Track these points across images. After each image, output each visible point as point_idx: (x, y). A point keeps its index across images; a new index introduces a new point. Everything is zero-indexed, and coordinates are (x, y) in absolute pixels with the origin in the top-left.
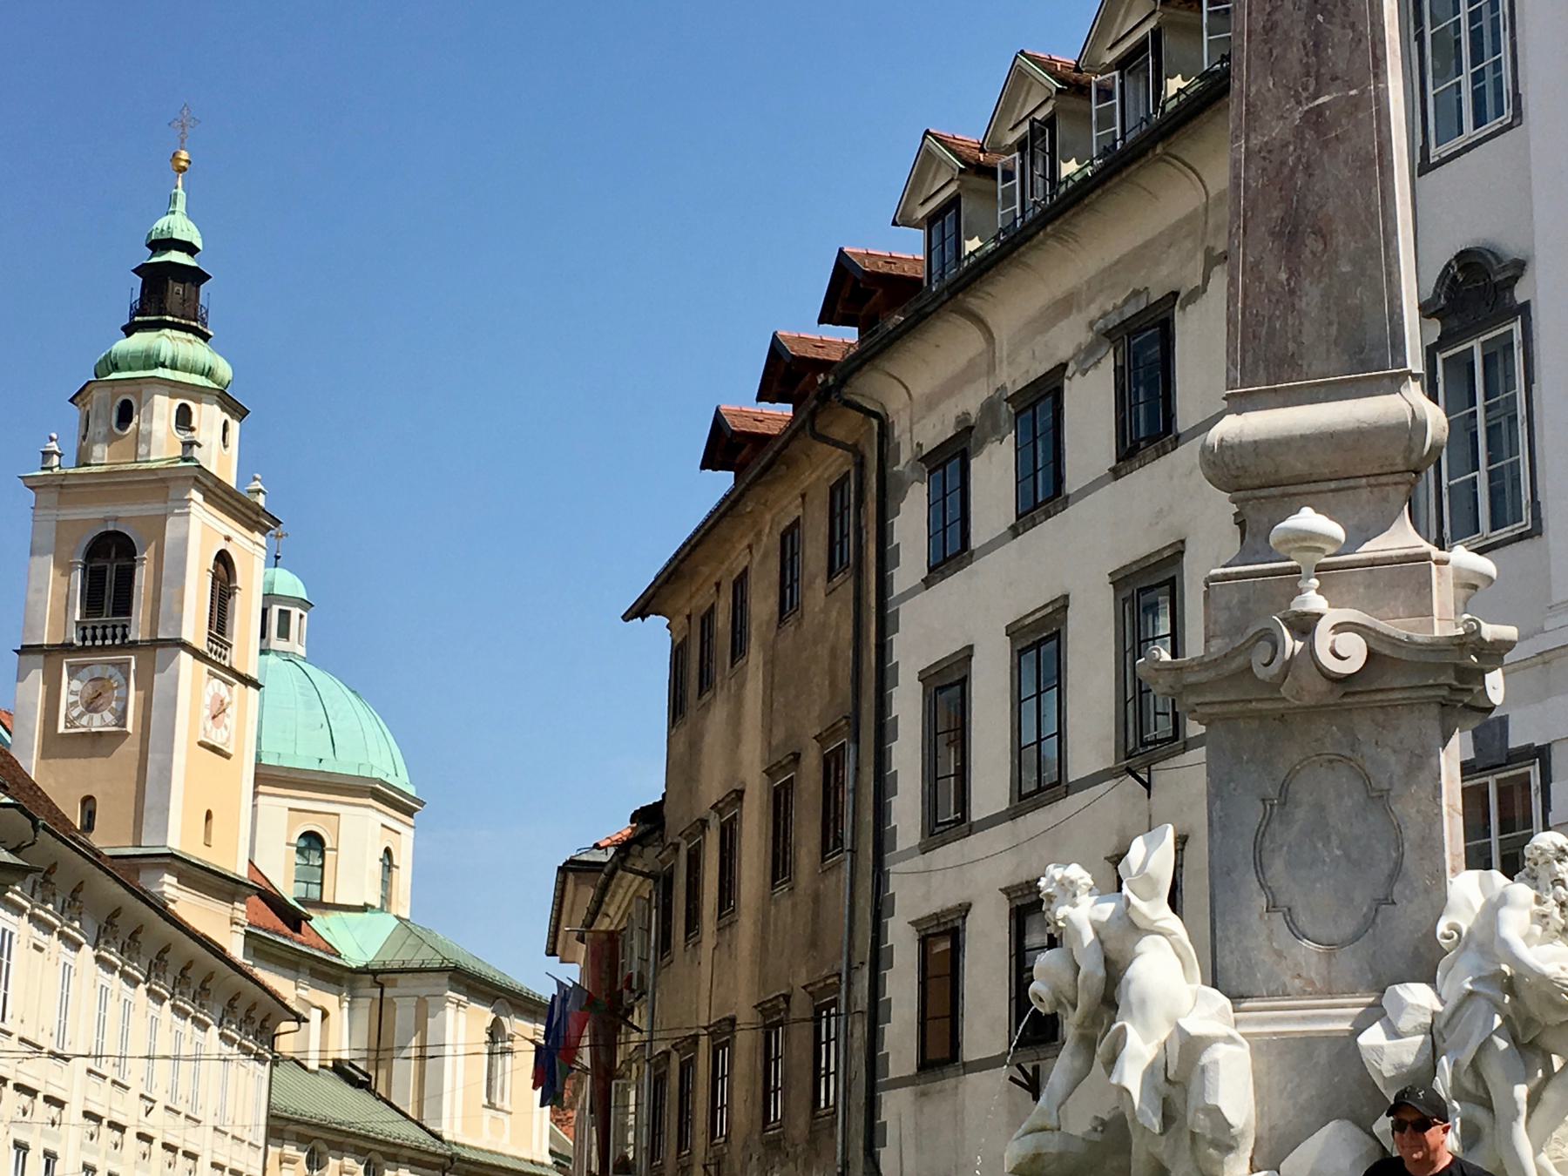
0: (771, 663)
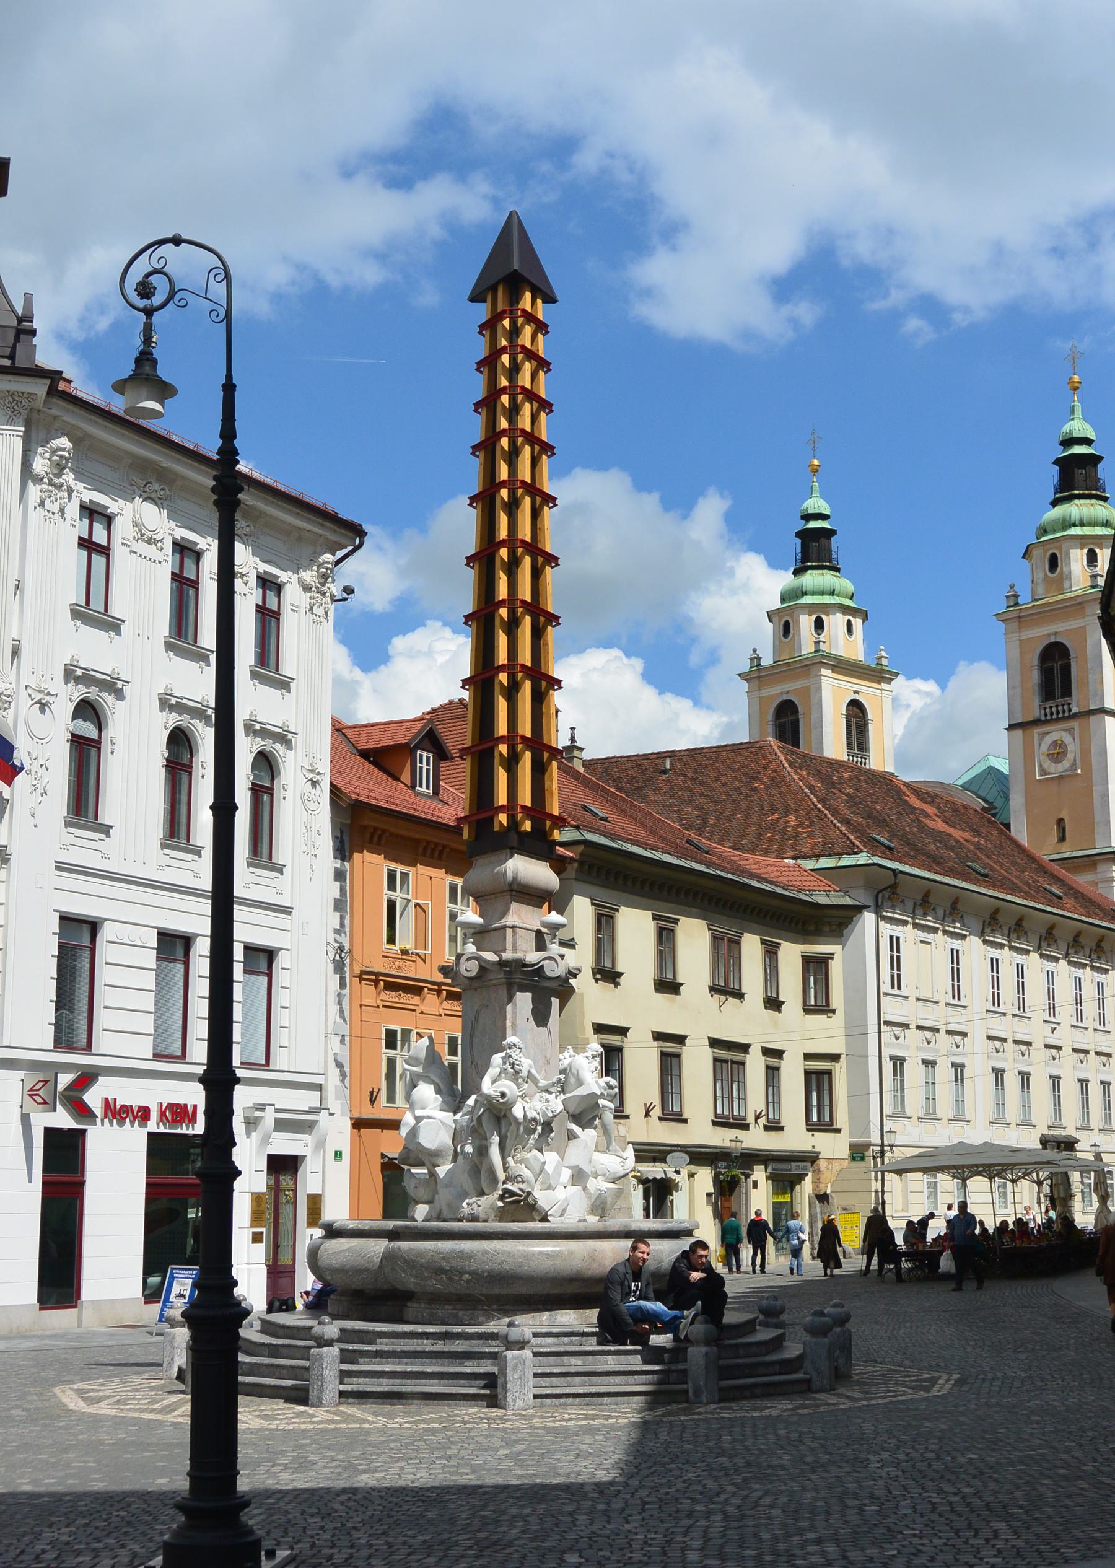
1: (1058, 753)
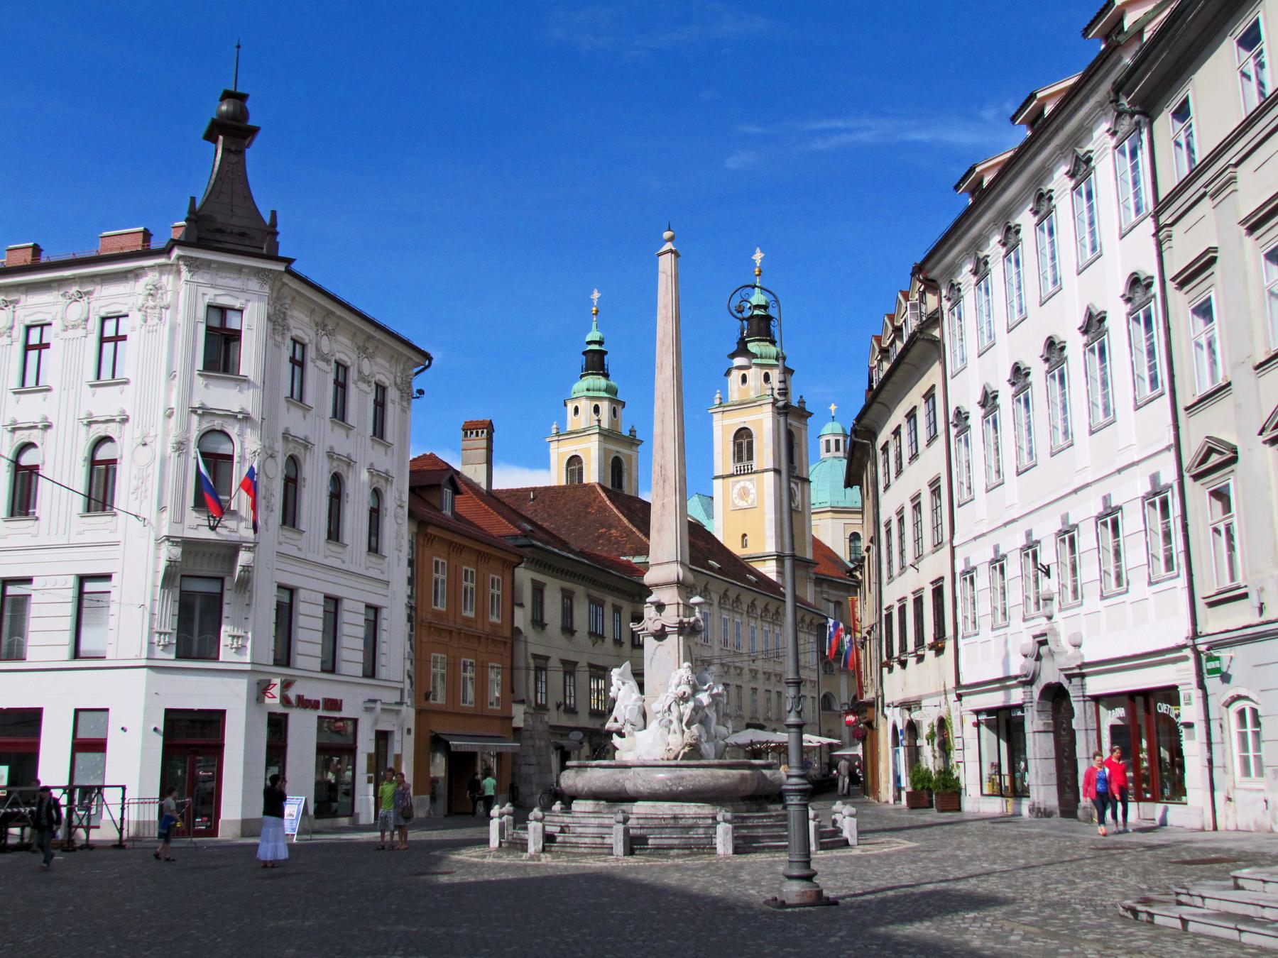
1: (744, 493)
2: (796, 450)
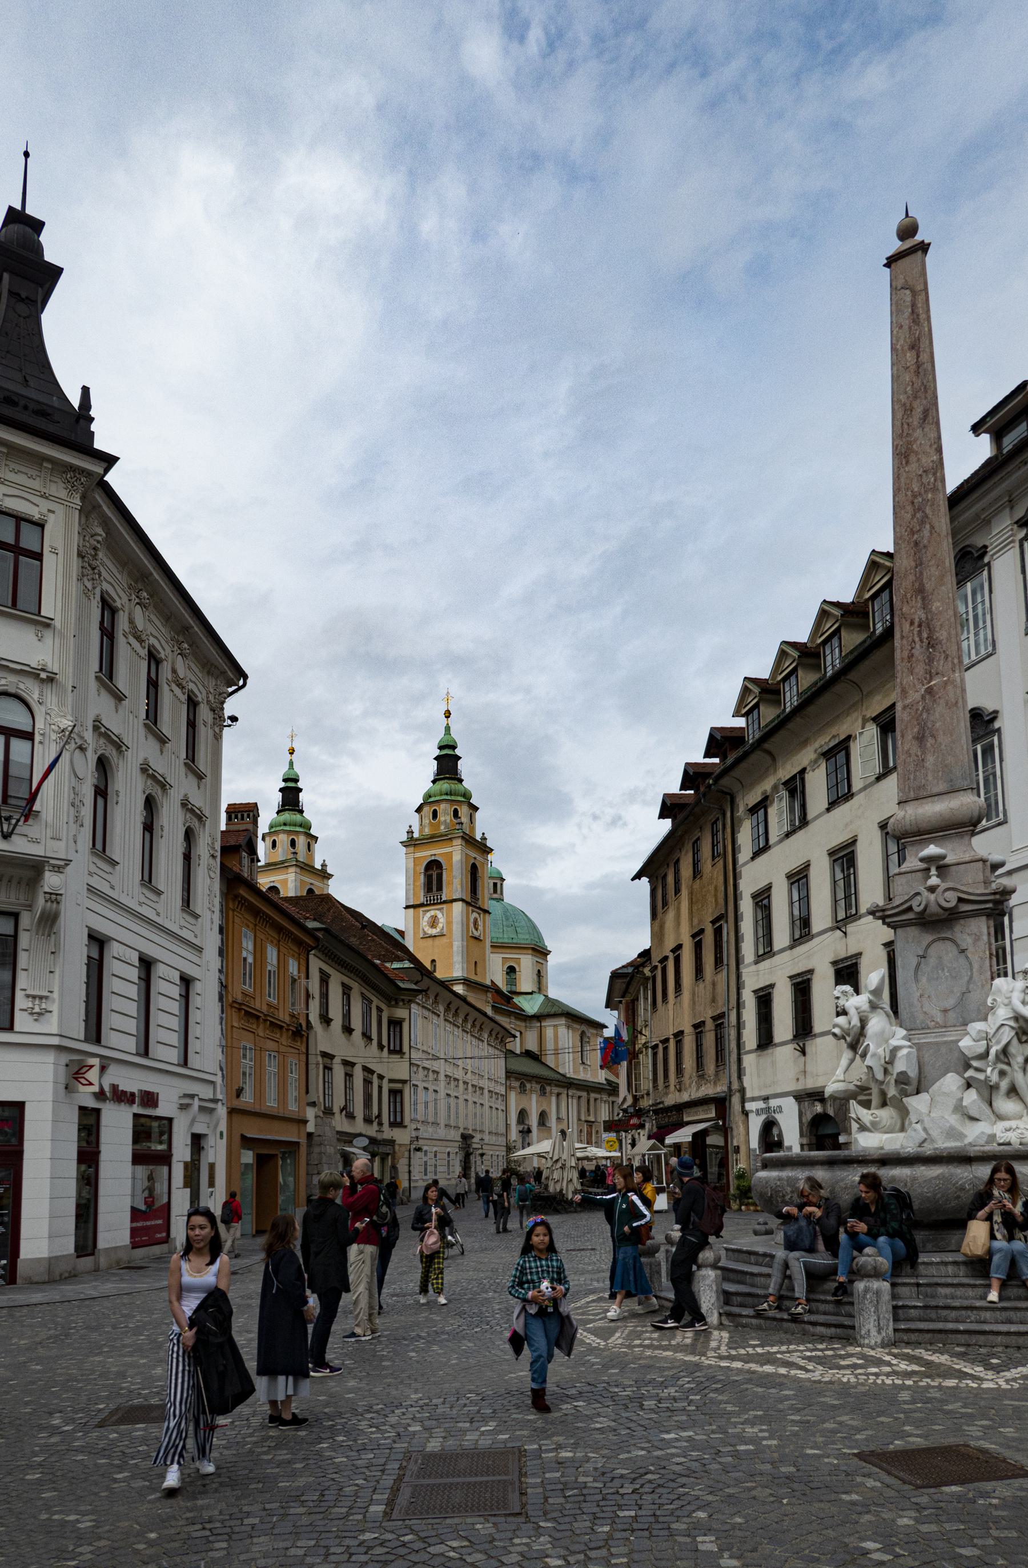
0: (691, 893)
2: (479, 883)
